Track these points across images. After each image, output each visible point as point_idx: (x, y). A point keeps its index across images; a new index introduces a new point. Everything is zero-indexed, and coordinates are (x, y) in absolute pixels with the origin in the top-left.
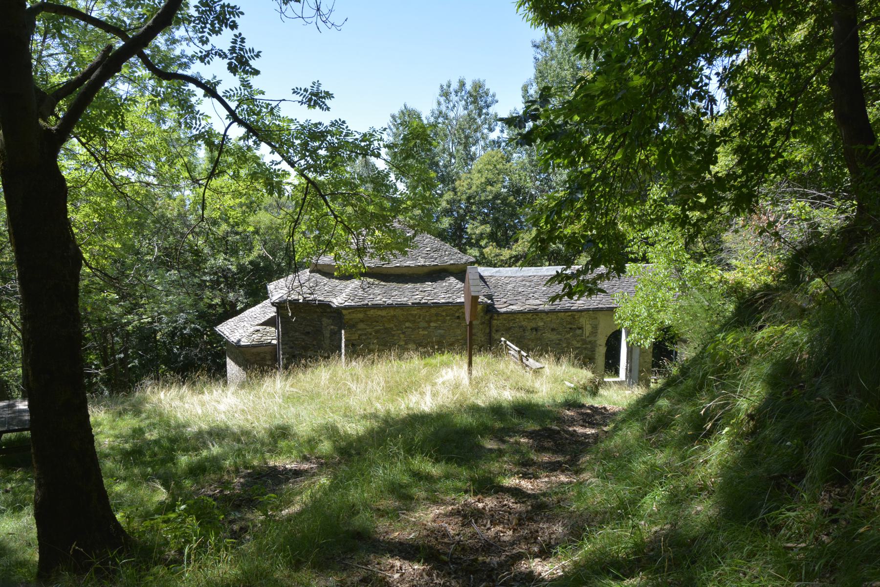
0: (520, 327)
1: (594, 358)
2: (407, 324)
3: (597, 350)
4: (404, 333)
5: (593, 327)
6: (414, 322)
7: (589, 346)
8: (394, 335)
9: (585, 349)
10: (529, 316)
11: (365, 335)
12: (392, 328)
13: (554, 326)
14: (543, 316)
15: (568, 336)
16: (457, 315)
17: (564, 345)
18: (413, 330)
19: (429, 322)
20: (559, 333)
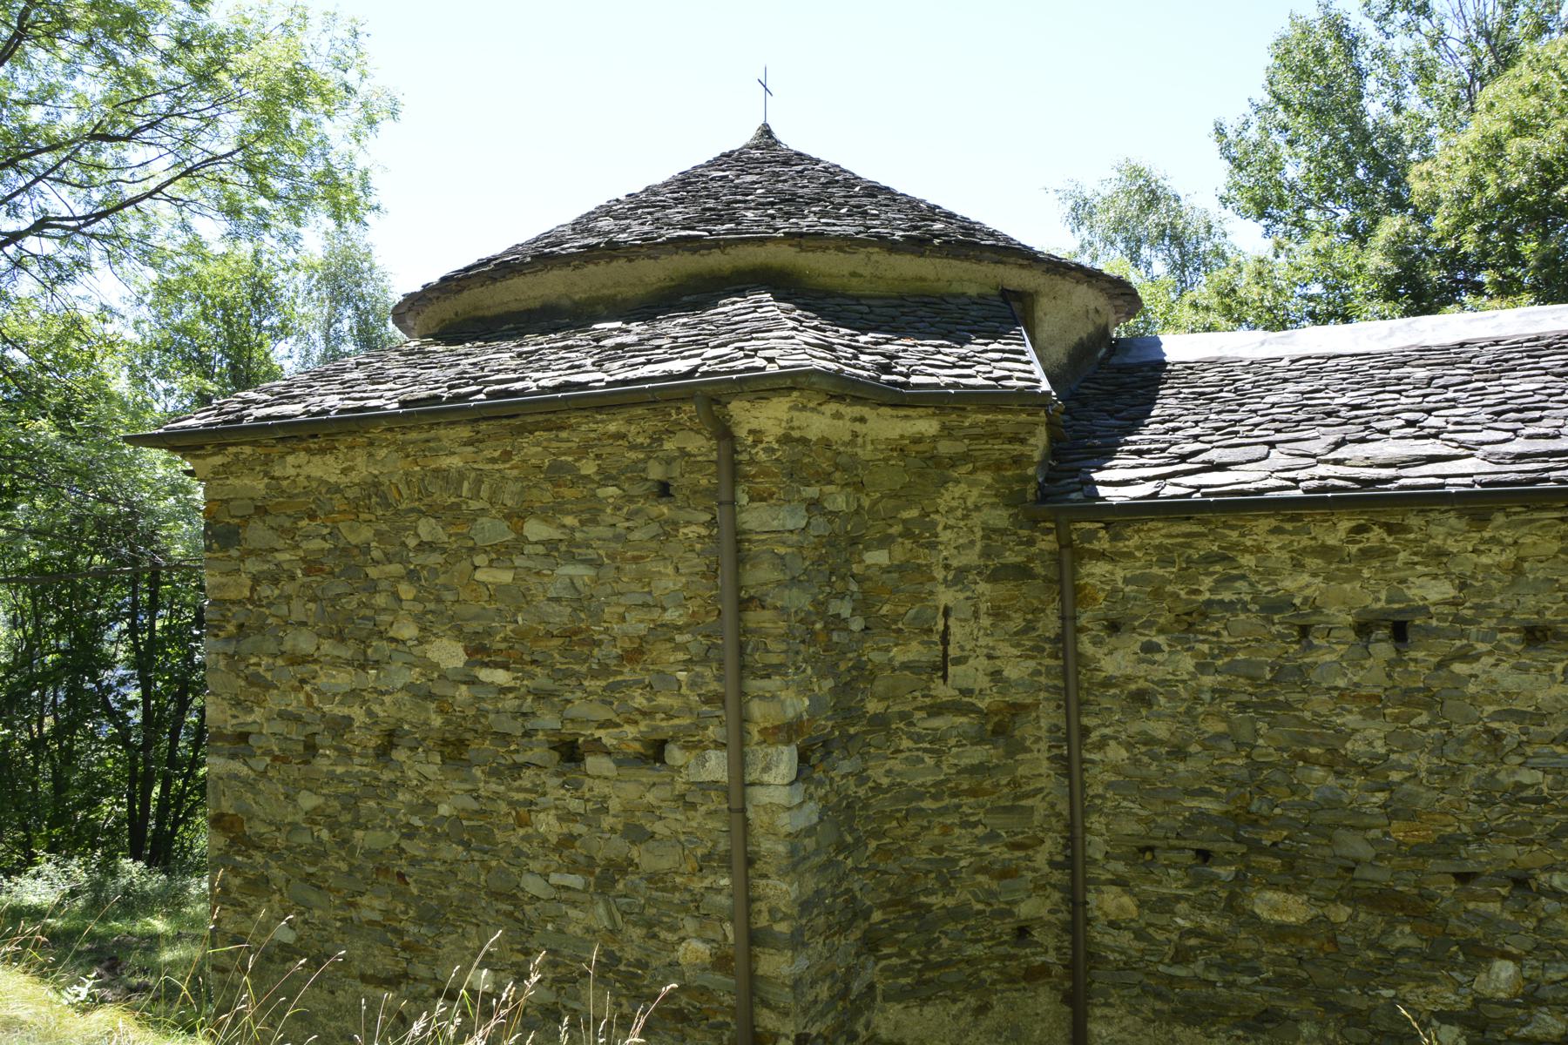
0: (1273, 607)
2: (427, 529)
4: (412, 576)
6: (451, 514)
8: (372, 587)
11: (275, 581)
12: (365, 549)
14: (1445, 531)
16: (656, 472)
18: (452, 557)
19: (516, 517)
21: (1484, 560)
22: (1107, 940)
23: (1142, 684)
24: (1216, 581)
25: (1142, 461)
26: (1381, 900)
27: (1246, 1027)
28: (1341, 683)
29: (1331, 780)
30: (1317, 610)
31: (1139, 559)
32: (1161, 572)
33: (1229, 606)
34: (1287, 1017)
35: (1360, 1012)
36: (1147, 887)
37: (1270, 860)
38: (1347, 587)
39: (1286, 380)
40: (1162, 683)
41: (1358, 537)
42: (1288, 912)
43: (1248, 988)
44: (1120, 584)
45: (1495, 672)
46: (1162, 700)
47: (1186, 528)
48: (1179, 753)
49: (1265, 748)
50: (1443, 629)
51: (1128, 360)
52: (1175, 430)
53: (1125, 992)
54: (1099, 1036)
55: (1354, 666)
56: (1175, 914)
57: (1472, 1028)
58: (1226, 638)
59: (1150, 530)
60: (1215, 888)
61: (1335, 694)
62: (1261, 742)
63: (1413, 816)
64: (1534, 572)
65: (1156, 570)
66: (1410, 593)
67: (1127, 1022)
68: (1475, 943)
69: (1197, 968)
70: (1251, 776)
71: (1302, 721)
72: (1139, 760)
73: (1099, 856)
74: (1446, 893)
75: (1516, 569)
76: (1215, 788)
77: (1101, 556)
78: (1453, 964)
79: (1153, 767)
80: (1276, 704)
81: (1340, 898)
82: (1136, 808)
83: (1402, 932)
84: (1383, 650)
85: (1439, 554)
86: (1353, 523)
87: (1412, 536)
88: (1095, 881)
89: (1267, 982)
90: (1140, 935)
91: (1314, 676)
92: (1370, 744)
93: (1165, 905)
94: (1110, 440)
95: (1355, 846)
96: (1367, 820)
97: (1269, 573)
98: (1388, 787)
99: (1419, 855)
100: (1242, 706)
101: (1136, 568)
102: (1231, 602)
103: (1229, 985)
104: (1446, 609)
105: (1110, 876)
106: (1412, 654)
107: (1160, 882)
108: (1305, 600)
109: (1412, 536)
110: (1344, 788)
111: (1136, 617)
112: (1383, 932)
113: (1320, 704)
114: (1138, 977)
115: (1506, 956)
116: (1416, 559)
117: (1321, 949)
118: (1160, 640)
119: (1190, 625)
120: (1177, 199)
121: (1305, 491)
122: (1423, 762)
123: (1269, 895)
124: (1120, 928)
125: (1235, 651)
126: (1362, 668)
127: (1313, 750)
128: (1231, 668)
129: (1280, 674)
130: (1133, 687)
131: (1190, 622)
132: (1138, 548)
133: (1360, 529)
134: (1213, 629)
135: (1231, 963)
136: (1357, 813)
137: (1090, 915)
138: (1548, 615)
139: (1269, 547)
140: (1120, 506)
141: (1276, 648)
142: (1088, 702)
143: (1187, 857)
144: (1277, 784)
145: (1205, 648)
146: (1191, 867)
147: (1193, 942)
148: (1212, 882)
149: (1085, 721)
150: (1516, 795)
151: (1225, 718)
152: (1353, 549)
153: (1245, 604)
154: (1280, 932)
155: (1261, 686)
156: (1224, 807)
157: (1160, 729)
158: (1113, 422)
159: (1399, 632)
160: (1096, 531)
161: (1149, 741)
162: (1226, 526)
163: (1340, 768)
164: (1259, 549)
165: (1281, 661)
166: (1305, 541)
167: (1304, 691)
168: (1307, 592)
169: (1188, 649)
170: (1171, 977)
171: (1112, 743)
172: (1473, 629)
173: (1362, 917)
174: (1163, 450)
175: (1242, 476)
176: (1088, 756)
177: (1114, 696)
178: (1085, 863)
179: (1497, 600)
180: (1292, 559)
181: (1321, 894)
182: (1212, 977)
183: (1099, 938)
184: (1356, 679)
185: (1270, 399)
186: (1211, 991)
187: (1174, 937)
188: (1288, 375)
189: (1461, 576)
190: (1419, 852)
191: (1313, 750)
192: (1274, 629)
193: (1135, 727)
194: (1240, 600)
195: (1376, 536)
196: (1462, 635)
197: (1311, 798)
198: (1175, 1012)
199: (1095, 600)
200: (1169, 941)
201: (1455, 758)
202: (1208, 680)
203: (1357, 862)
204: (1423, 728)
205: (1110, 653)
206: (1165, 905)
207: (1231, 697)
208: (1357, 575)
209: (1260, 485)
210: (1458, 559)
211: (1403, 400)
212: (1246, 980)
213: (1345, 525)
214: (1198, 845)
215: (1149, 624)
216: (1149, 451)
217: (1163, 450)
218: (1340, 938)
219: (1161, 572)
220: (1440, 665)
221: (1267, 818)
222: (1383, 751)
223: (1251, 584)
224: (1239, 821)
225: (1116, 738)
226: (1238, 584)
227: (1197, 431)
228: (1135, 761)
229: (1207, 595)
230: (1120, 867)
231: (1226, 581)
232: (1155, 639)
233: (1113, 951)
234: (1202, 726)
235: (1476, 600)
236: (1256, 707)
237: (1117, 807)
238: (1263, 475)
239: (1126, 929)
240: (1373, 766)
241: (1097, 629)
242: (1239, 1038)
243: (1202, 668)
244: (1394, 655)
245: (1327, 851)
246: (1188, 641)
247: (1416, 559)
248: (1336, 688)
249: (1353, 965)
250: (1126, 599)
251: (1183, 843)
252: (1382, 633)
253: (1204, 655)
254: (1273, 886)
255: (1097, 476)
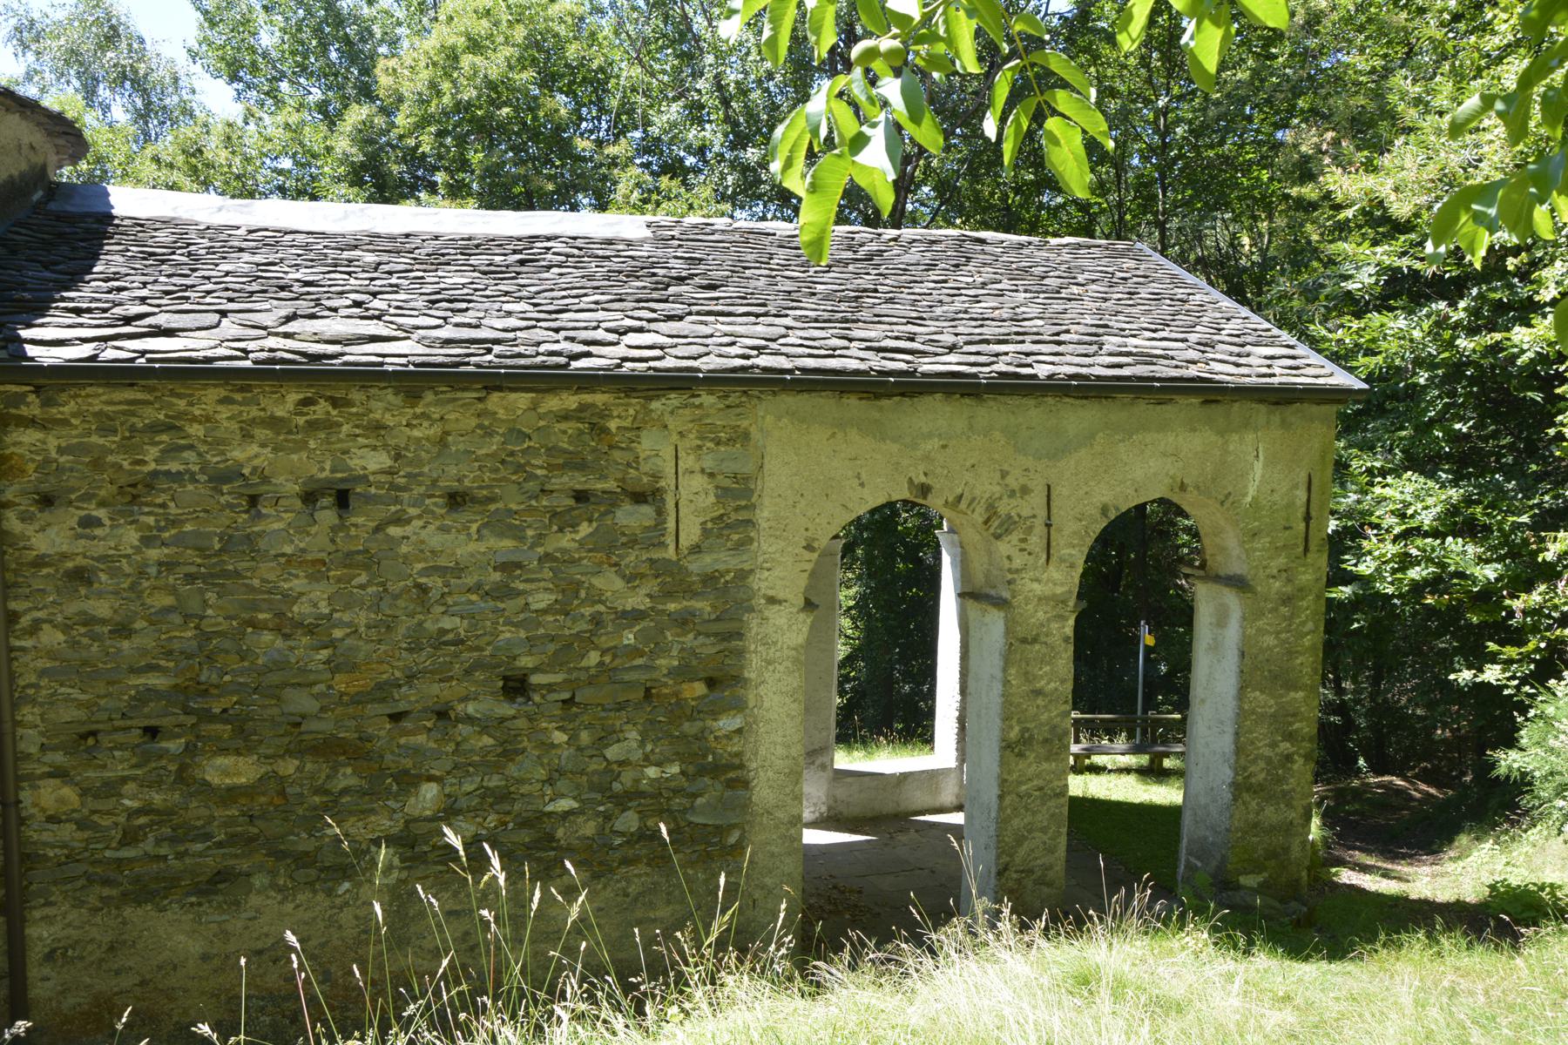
0: (220, 478)
1: (738, 680)
3: (753, 624)
5: (723, 493)
7: (703, 606)
9: (683, 621)
10: (285, 403)
13: (454, 474)
14: (384, 406)
15: (566, 541)
17: (541, 600)
20: (500, 525)
21: (416, 433)
22: (46, 837)
23: (80, 561)
24: (162, 451)
25: (80, 320)
26: (328, 749)
27: (200, 893)
28: (288, 549)
29: (279, 643)
30: (265, 480)
31: (76, 427)
32: (101, 441)
33: (176, 477)
34: (240, 874)
35: (307, 853)
36: (91, 774)
37: (219, 727)
38: (295, 457)
39: (241, 250)
40: (103, 558)
41: (305, 410)
42: (239, 774)
43: (201, 855)
44: (54, 455)
45: (424, 533)
46: (103, 577)
47: (130, 394)
48: (123, 630)
49: (214, 618)
50: (380, 496)
51: (69, 208)
52: (120, 289)
53: (69, 886)
54: (40, 939)
55: (300, 533)
56: (121, 796)
57: (403, 846)
58: (173, 509)
59: (88, 396)
60: (163, 762)
61: (283, 560)
62: (210, 612)
63: (354, 668)
64: (457, 445)
65: (94, 439)
66: (352, 463)
67: (73, 916)
68: (406, 772)
69: (148, 846)
70: (200, 647)
71: (252, 589)
72: (78, 643)
73: (33, 750)
74: (382, 733)
75: (442, 442)
76: (162, 663)
77: (32, 422)
78: (389, 794)
79: (95, 648)
80: (225, 574)
81: (289, 753)
82: (75, 693)
83: (344, 775)
84: (327, 516)
85: (378, 427)
86: (301, 396)
87: (354, 410)
88: (31, 777)
89: (220, 845)
90: (82, 825)
91: (262, 544)
92: (315, 605)
93: (111, 789)
94: (43, 294)
95: (302, 702)
96: (312, 677)
97: (219, 444)
98: (332, 644)
99: (359, 703)
100: (190, 578)
101: (72, 437)
102: (179, 473)
103: (180, 856)
104: (383, 478)
105: (47, 769)
106: (353, 520)
107: (104, 767)
108: (255, 469)
109: (354, 410)
110: (291, 649)
111: (73, 490)
112: (328, 777)
113: (269, 571)
114: (82, 868)
115: (431, 779)
116: (358, 431)
117: (271, 803)
118: (101, 513)
119: (135, 497)
120: (142, 41)
121: (255, 362)
122: (362, 618)
123: (220, 761)
124: (60, 822)
125: (183, 522)
126: (308, 534)
127: (261, 616)
128: (179, 540)
129: (228, 542)
130: (70, 565)
131: (134, 494)
132: (74, 415)
133: (307, 402)
134: (159, 501)
135: (183, 834)
136: (303, 671)
137: (24, 814)
138: (467, 483)
139: (218, 417)
140: (52, 368)
141: (225, 518)
142: (16, 585)
143: (135, 737)
144: (227, 652)
145: (151, 520)
146: (137, 746)
147: (142, 820)
148: (161, 757)
149: (13, 605)
150: (440, 640)
151: (173, 591)
152: (301, 420)
153: (193, 474)
154: (231, 795)
155: (210, 556)
156: (173, 681)
157: (102, 608)
158: (48, 274)
159: (343, 500)
160: (24, 395)
161: (89, 620)
162: (173, 394)
163: (287, 631)
164: (208, 419)
165: (230, 531)
166: (254, 412)
167: (253, 559)
168: (256, 462)
169: (132, 523)
170: (119, 861)
171: (45, 626)
172: (406, 495)
173: (309, 766)
174: (105, 310)
175: (190, 344)
176: (18, 643)
177: (48, 575)
178: (17, 759)
179: (426, 470)
180: (242, 429)
181: (270, 751)
182: (163, 852)
183: (35, 837)
184: (302, 545)
185: (225, 267)
186: (162, 865)
187: (122, 819)
188: (245, 245)
189: (396, 448)
190: (359, 700)
191: (261, 616)
192: (223, 500)
193: (72, 608)
194: (187, 471)
195: (321, 409)
196: (397, 501)
197: (260, 661)
198: (124, 895)
199: (23, 471)
200: (116, 824)
201: (389, 612)
202: (154, 554)
203: (303, 717)
204: (362, 587)
205: (43, 529)
206: (111, 789)
207: (178, 570)
208: (303, 446)
209: (209, 353)
210: (395, 432)
211: (352, 281)
212: (199, 847)
213: (293, 397)
214: (146, 723)
215: (87, 497)
216: (89, 310)
217: (105, 310)
218: (288, 790)
219: (101, 441)
220: (377, 529)
221: (217, 687)
222: (327, 611)
223: (200, 455)
224: (188, 694)
225: (51, 622)
226: (186, 454)
227: (145, 292)
228: (74, 644)
229: (153, 466)
230: (58, 758)
231: (172, 451)
232: (94, 513)
233: (53, 847)
234: (148, 601)
235: (409, 470)
236: (204, 578)
237: (52, 695)
238: (212, 343)
239: (67, 821)
240: (318, 626)
241: (25, 504)
242: (192, 904)
243: (147, 541)
244: (337, 521)
245: (275, 711)
246: (132, 513)
247: (358, 431)
248: (283, 555)
249: (300, 812)
250: (60, 470)
251: (129, 723)
252: (327, 501)
253: (150, 528)
254: (224, 751)
255: (25, 333)
